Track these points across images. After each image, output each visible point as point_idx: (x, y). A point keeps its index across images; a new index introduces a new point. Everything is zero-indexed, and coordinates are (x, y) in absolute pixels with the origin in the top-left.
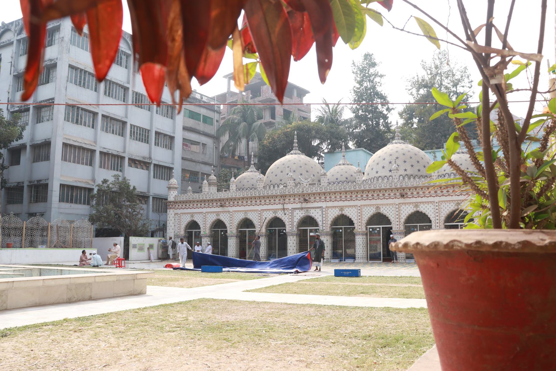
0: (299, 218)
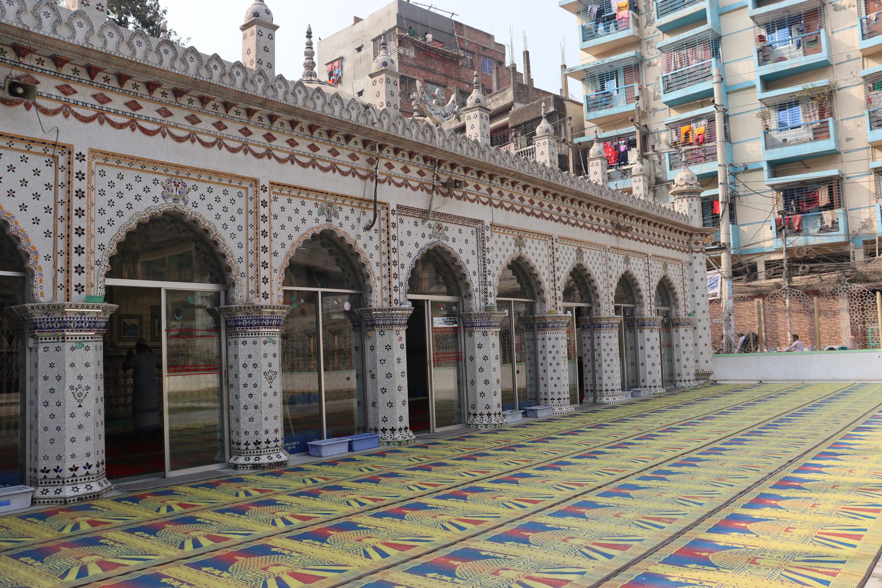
0: (415, 252)
